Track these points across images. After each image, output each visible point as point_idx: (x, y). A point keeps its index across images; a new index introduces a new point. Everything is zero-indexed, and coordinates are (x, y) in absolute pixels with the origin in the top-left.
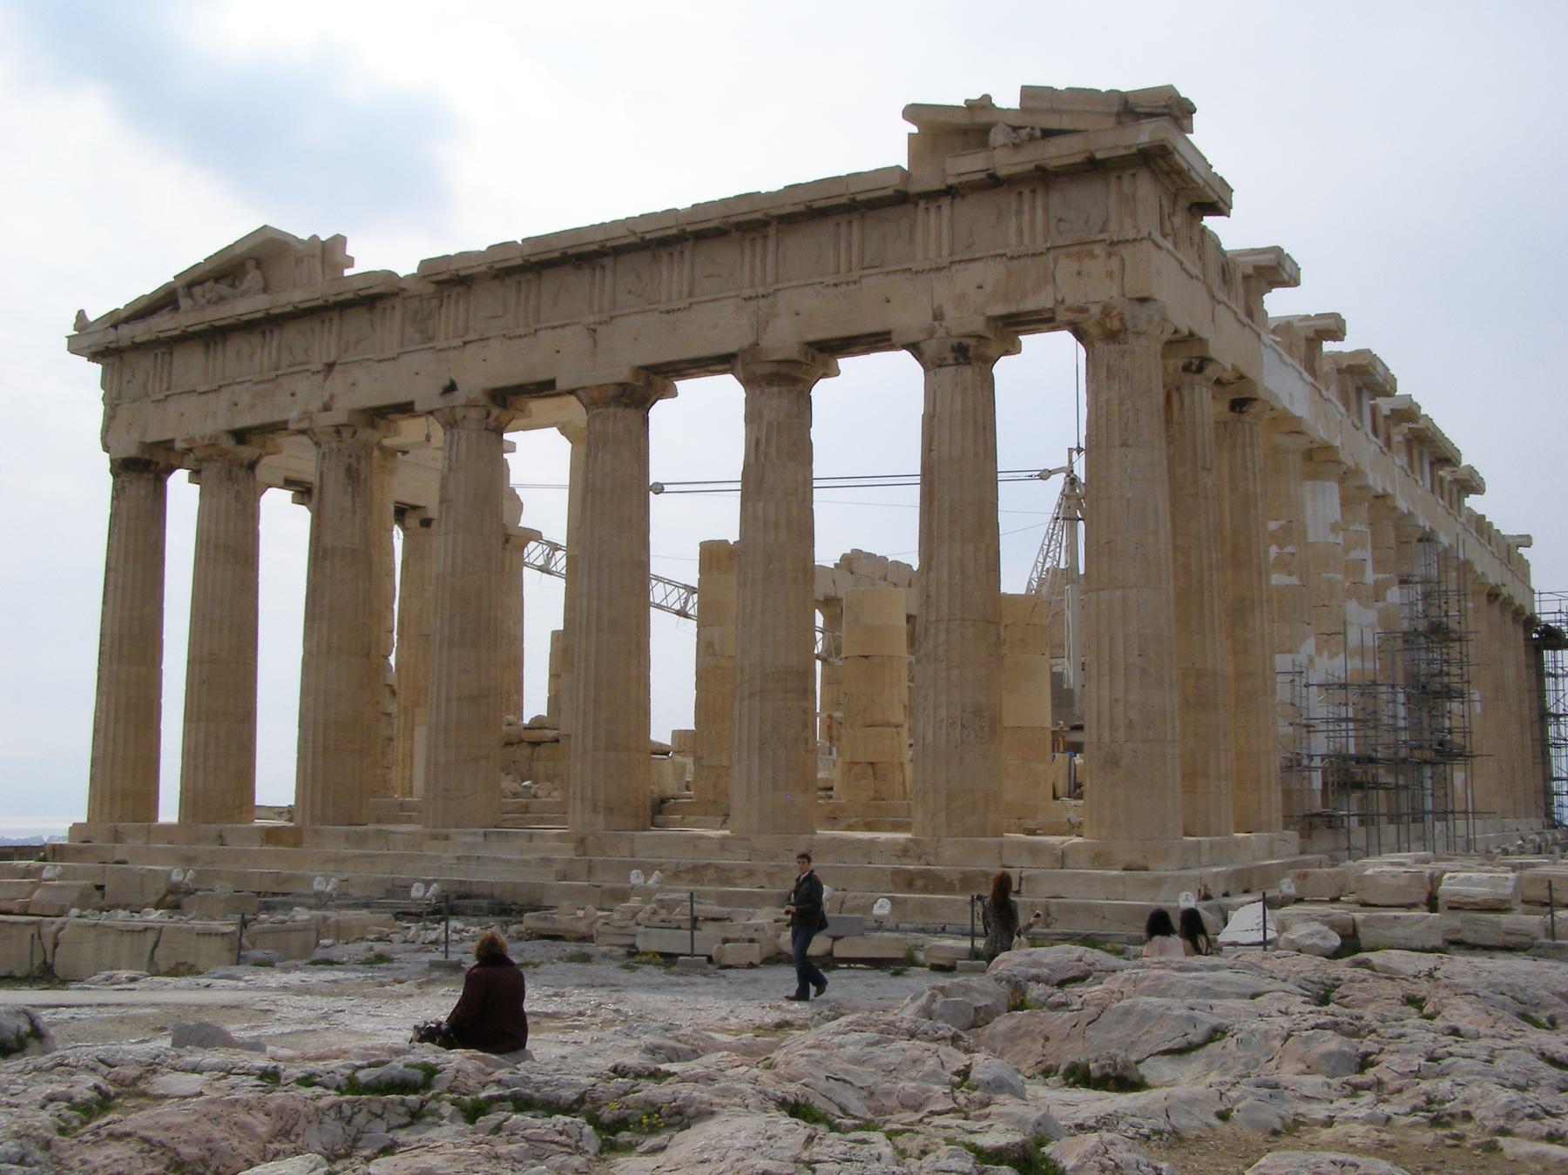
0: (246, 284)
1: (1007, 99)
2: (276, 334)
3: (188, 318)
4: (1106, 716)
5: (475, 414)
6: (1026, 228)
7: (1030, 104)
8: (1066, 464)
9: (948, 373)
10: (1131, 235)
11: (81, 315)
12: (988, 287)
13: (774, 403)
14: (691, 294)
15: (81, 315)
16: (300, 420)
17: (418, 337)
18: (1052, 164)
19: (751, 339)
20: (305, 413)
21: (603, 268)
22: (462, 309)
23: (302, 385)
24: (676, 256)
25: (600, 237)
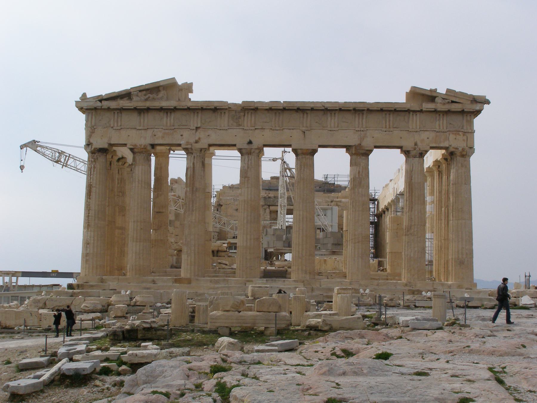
0: (161, 94)
1: (442, 90)
2: (173, 114)
3: (137, 102)
5: (257, 151)
7: (448, 93)
8: (281, 156)
10: (470, 131)
11: (84, 95)
13: (364, 161)
14: (338, 127)
15: (84, 95)
16: (187, 145)
17: (235, 124)
18: (453, 110)
19: (359, 142)
21: (307, 113)
22: (253, 118)
23: (186, 134)
24: (333, 114)
25: (312, 106)
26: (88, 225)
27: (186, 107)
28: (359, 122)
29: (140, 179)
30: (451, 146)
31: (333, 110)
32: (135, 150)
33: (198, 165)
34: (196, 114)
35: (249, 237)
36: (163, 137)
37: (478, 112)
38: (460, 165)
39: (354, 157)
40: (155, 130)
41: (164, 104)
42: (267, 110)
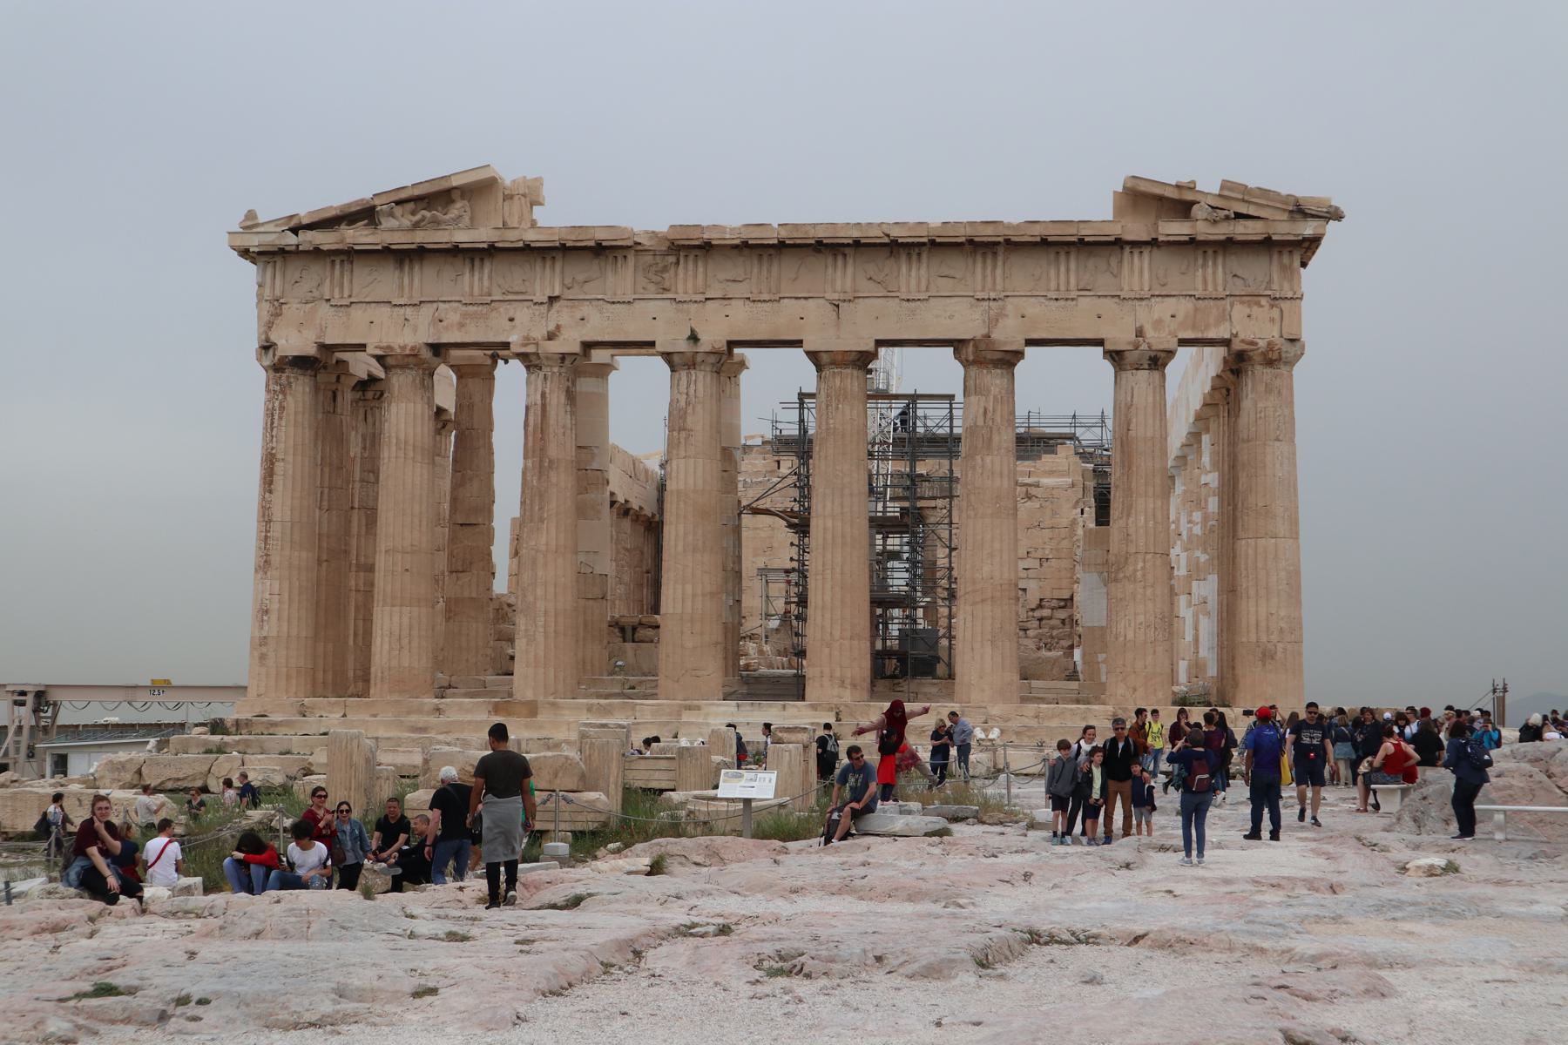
1: (1209, 185)
4: (1263, 624)
5: (712, 359)
6: (1210, 278)
7: (1226, 193)
9: (1143, 375)
10: (1290, 295)
11: (251, 215)
12: (1180, 317)
14: (927, 290)
15: (251, 215)
16: (525, 345)
17: (652, 287)
19: (985, 331)
20: (527, 338)
21: (845, 255)
22: (701, 269)
23: (523, 314)
24: (914, 257)
25: (856, 234)
26: (264, 565)
27: (521, 244)
28: (984, 277)
29: (402, 437)
30: (1236, 336)
31: (913, 245)
32: (390, 361)
33: (557, 399)
34: (548, 264)
35: (689, 588)
36: (461, 325)
37: (1313, 243)
38: (1262, 388)
39: (973, 370)
40: (442, 305)
41: (463, 237)
42: (735, 247)
